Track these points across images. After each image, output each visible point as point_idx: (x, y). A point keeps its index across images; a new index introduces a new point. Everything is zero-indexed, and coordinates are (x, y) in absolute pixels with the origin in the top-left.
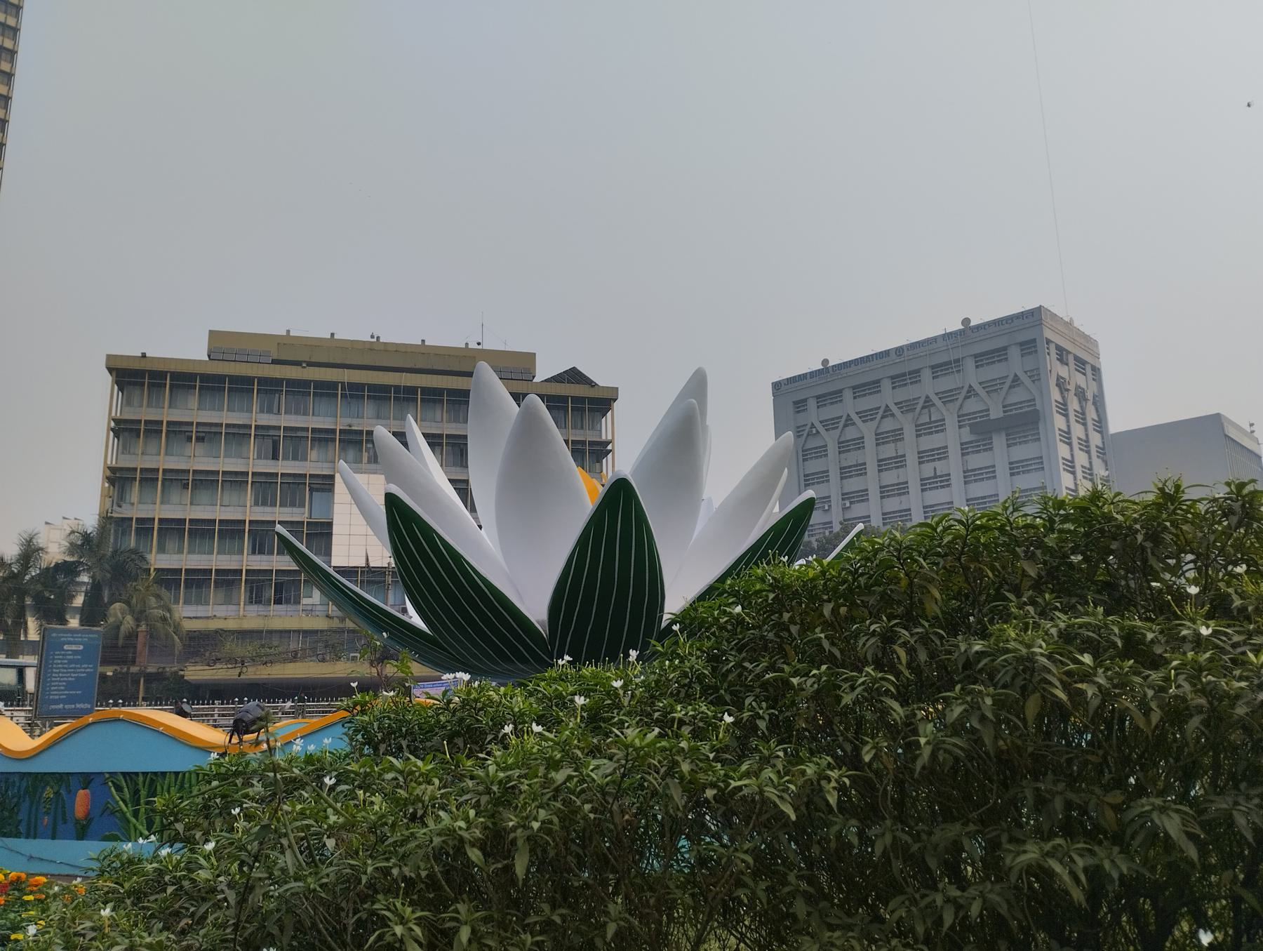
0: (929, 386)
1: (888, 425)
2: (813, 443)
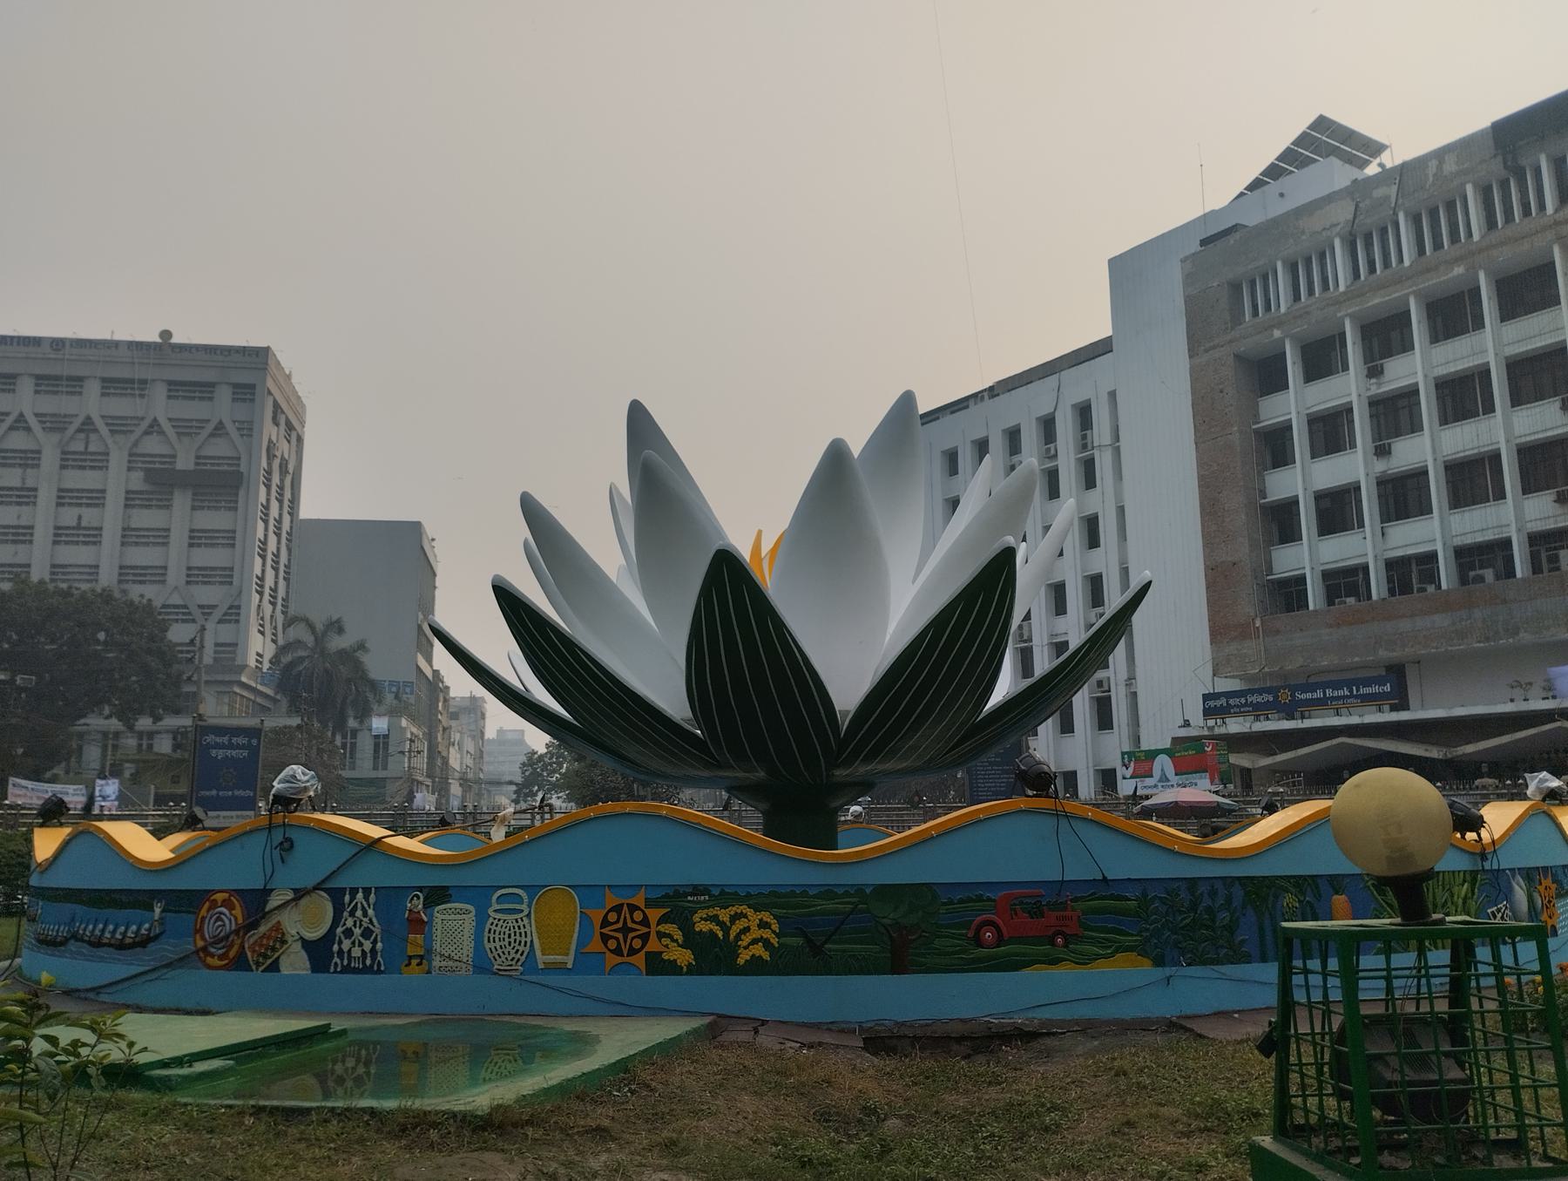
0: (92, 403)
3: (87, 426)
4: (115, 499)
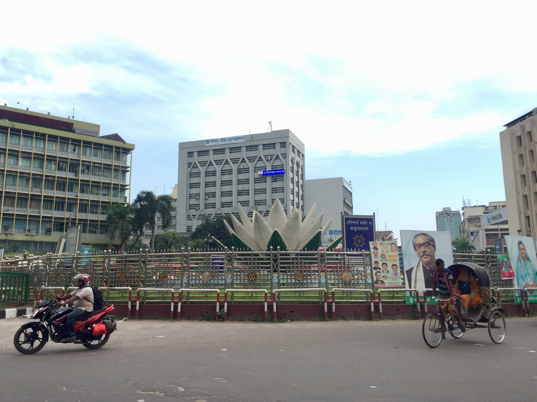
1: (227, 167)
2: (195, 171)
3: (243, 161)
4: (252, 181)
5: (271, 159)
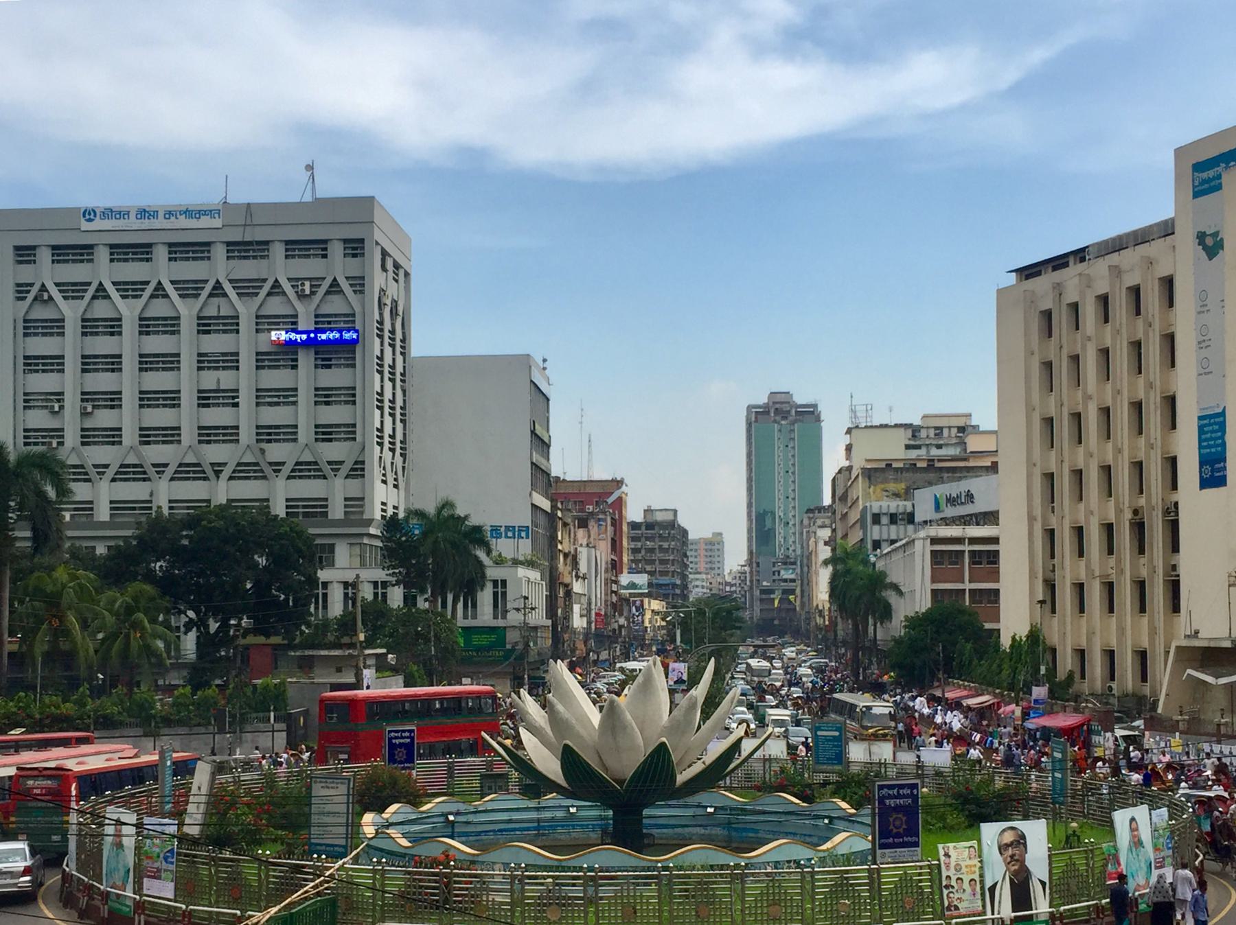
1: (159, 309)
2: (40, 313)
4: (247, 361)
5: (313, 293)
